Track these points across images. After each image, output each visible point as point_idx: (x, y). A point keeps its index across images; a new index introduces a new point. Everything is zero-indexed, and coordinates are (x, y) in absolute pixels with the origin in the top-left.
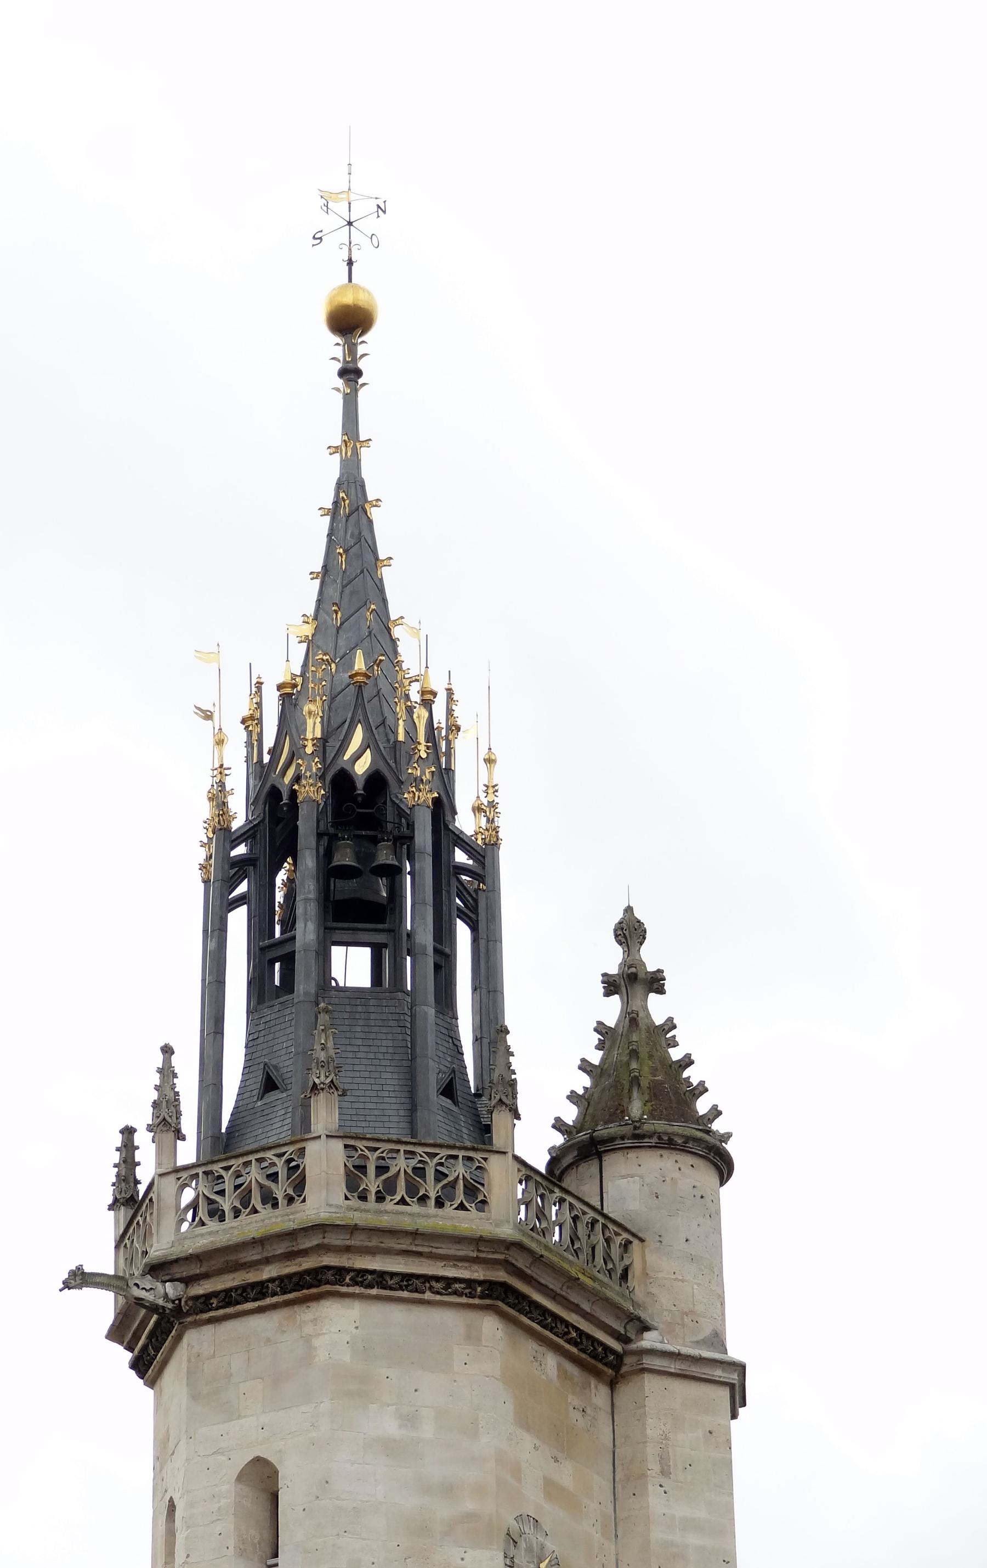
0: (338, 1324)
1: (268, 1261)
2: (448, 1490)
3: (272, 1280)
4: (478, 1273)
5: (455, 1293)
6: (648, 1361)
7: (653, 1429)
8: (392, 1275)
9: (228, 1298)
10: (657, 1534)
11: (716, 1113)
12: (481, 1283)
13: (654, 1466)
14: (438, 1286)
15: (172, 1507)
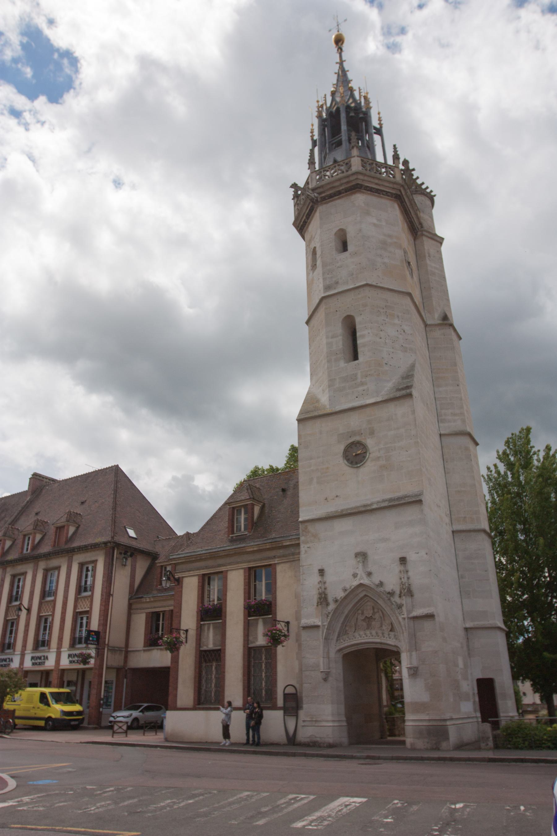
0: (360, 199)
1: (341, 185)
2: (390, 236)
3: (343, 189)
4: (394, 192)
5: (388, 196)
6: (425, 233)
7: (426, 248)
8: (374, 188)
9: (331, 196)
10: (429, 268)
11: (431, 191)
12: (395, 194)
13: (427, 255)
14: (384, 193)
15: (314, 252)
